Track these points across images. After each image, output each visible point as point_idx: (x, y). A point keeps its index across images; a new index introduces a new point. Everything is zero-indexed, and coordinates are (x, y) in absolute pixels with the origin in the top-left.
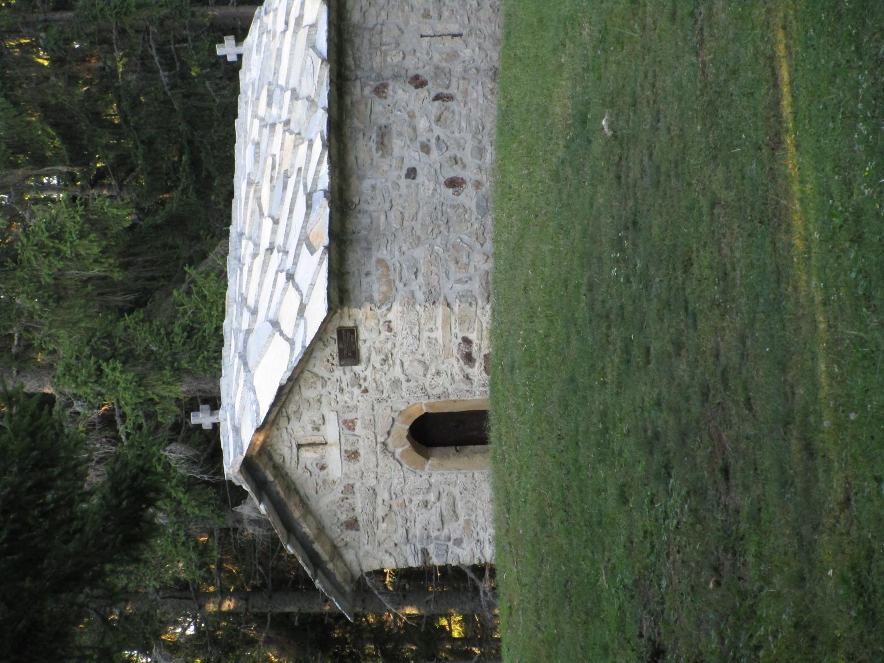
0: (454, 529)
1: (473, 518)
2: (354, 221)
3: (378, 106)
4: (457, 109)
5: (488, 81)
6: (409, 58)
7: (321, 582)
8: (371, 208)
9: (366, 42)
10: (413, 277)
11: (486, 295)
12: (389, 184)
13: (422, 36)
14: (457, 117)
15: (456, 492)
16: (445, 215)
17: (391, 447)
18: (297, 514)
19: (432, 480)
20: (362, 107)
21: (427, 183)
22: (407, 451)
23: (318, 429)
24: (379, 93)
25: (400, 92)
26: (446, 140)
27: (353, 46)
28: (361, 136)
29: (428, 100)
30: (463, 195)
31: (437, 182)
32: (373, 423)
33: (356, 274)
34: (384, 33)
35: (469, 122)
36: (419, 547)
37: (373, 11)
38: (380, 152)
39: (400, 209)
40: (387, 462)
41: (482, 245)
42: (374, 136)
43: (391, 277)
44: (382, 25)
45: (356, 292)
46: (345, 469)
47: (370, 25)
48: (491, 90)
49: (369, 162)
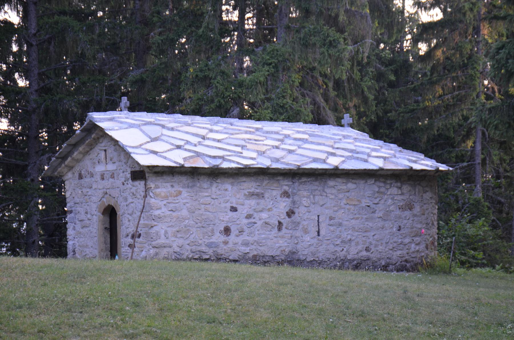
0: (78, 227)
1: (82, 236)
2: (206, 180)
3: (276, 193)
4: (273, 233)
5: (290, 249)
6: (306, 209)
7: (55, 161)
8: (214, 189)
9: (316, 187)
10: (170, 209)
11: (157, 246)
12: (228, 198)
13: (318, 216)
14: (268, 233)
15: (90, 228)
16: (207, 226)
17: (106, 196)
18: (81, 149)
19: (94, 216)
20: (275, 185)
21: (227, 217)
22: (105, 204)
23: (111, 160)
25: (285, 204)
27: (314, 181)
28: (258, 184)
30: (219, 234)
31: (228, 222)
32: (113, 188)
34: (320, 197)
35: (265, 239)
36: (73, 209)
37: (334, 191)
38: (247, 194)
39: (212, 203)
40: (100, 193)
41: (188, 244)
42: (258, 191)
43: (170, 198)
44: (326, 196)
45: (161, 180)
46: (98, 174)
47: (325, 190)
49: (242, 188)
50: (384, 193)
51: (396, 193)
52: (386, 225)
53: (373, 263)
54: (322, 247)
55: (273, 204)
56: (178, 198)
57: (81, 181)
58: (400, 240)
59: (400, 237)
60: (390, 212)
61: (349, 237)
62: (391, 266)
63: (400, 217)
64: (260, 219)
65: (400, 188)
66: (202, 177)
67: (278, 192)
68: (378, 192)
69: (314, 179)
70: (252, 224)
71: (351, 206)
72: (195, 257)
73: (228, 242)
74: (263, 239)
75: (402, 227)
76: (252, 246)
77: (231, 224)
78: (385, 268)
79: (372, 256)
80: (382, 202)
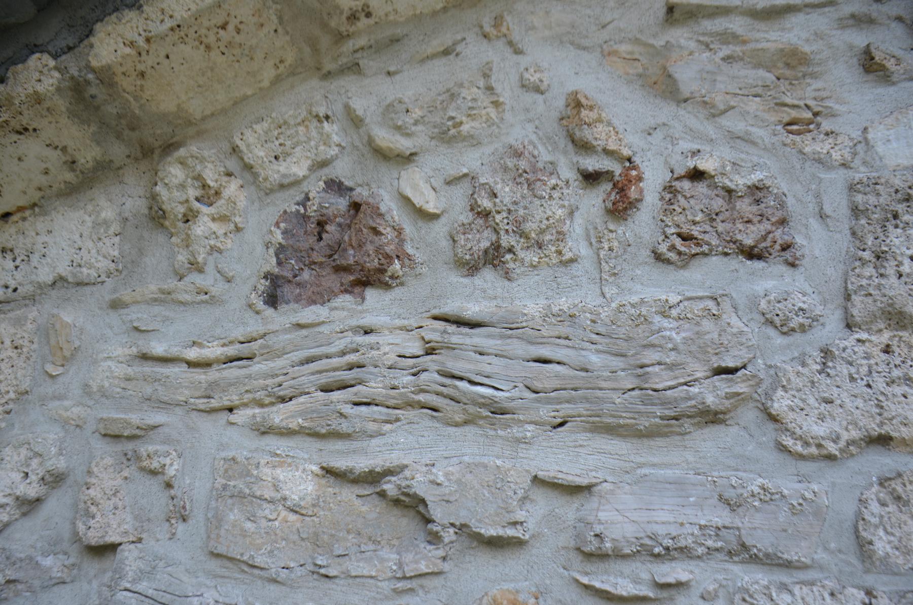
57: (338, 315)
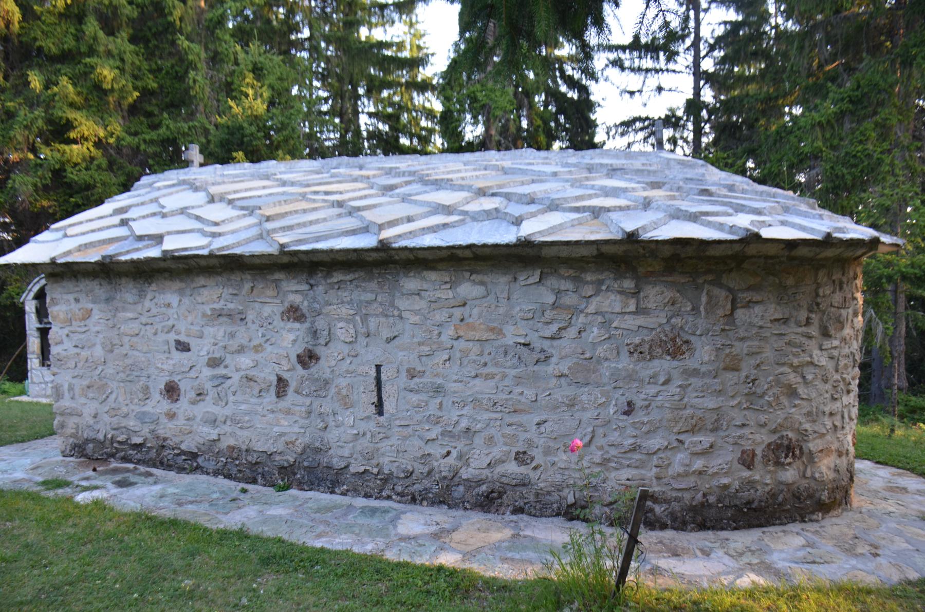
3: (272, 308)
5: (307, 440)
6: (346, 349)
8: (147, 304)
9: (370, 296)
13: (378, 367)
14: (253, 400)
16: (137, 379)
21: (171, 362)
24: (289, 311)
25: (291, 337)
26: (224, 385)
27: (364, 280)
29: (277, 369)
31: (171, 373)
33: (77, 289)
34: (383, 319)
39: (142, 333)
42: (231, 306)
43: (74, 323)
44: (401, 317)
45: (59, 289)
47: (397, 302)
48: (293, 443)
50: (575, 311)
51: (618, 310)
52: (584, 398)
53: (537, 495)
54: (390, 443)
55: (263, 336)
56: (87, 322)
58: (631, 441)
59: (630, 431)
60: (599, 362)
61: (464, 424)
62: (598, 507)
63: (631, 377)
64: (237, 371)
65: (636, 294)
66: (123, 281)
67: (275, 309)
68: (554, 306)
69: (362, 274)
70: (220, 380)
71: (471, 344)
72: (119, 439)
73: (175, 414)
74: (246, 414)
75: (639, 402)
76: (224, 427)
77: (179, 377)
78: (571, 513)
79: (534, 476)
80: (572, 332)
